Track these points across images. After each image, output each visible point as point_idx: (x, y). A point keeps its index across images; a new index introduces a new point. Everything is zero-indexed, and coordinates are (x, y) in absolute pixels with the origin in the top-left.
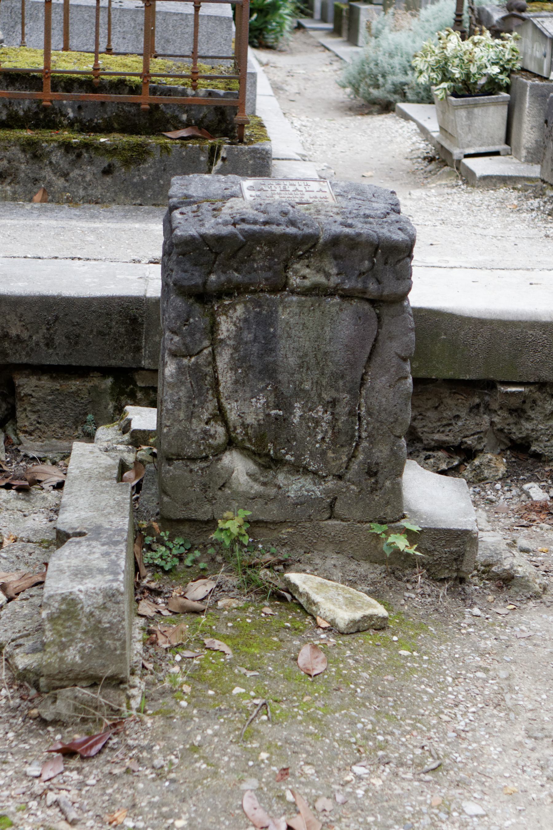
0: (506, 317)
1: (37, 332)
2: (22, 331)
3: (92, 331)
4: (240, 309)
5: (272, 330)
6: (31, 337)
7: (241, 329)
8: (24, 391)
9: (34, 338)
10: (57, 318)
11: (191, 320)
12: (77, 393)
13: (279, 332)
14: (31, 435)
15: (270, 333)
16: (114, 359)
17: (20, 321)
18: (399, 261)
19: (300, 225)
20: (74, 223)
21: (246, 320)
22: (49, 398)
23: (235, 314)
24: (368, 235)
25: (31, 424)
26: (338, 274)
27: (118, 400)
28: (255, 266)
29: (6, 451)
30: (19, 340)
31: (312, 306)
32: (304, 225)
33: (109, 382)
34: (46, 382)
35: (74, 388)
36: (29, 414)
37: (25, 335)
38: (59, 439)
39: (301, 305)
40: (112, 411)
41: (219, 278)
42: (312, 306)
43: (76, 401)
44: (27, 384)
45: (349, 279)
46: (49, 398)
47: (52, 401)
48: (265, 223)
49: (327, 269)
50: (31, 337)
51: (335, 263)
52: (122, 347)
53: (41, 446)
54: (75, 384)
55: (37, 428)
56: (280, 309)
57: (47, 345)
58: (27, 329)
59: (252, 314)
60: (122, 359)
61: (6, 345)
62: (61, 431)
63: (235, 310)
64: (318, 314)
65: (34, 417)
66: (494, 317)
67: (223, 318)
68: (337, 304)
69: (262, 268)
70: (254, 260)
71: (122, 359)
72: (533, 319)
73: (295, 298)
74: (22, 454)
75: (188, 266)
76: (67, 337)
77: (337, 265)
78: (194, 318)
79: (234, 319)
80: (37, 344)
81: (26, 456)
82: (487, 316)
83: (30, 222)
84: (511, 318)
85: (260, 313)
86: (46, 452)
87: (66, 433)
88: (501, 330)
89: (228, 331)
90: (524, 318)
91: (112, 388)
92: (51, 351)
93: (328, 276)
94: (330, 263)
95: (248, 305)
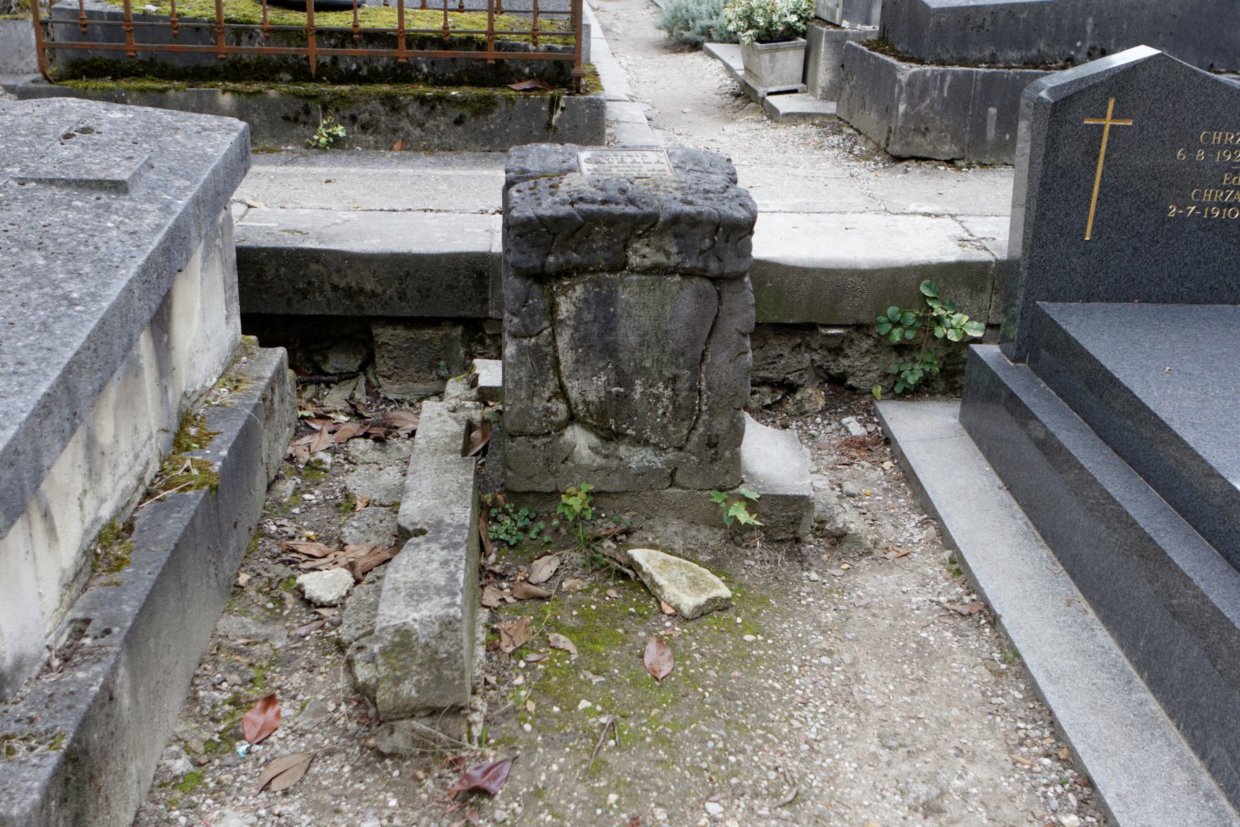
0: (827, 266)
4: (579, 289)
10: (408, 273)
12: (430, 341)
13: (619, 311)
14: (389, 378)
18: (740, 238)
20: (429, 171)
21: (585, 300)
24: (710, 214)
27: (468, 346)
29: (367, 394)
30: (373, 294)
33: (459, 330)
34: (401, 332)
35: (427, 337)
37: (379, 289)
39: (641, 284)
41: (557, 259)
44: (384, 334)
47: (407, 348)
48: (604, 202)
51: (675, 241)
54: (428, 333)
56: (620, 289)
57: (400, 298)
61: (362, 299)
63: (575, 290)
64: (658, 293)
65: (392, 363)
66: (817, 266)
67: (563, 298)
69: (601, 249)
70: (593, 240)
73: (635, 277)
77: (677, 244)
80: (391, 298)
81: (385, 398)
82: (810, 265)
83: (389, 171)
84: (832, 266)
85: (599, 293)
88: (823, 278)
90: (844, 266)
91: (462, 336)
93: (668, 255)
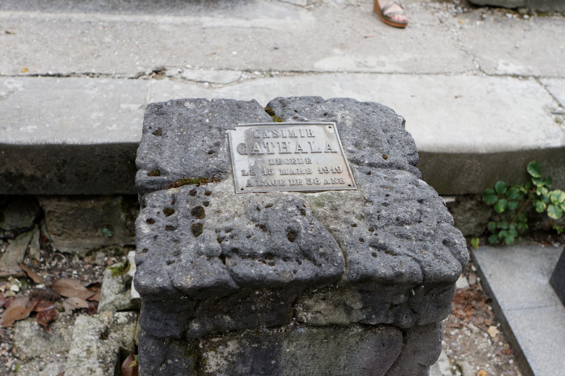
0: (451, 151)
1: (49, 172)
2: (35, 172)
3: (98, 170)
4: (232, 346)
5: (273, 362)
6: (44, 176)
7: (234, 363)
8: (47, 209)
9: (47, 176)
10: (65, 162)
11: (170, 362)
12: (93, 209)
13: (282, 363)
14: (60, 235)
15: (271, 365)
16: (121, 189)
17: (32, 164)
18: (444, 291)
19: (316, 257)
20: (99, 16)
21: (240, 355)
22: (71, 212)
23: (227, 350)
24: (412, 274)
25: (58, 230)
26: (361, 310)
27: (128, 211)
28: (253, 308)
29: (41, 248)
30: (32, 178)
31: (326, 338)
32: (322, 255)
33: (119, 200)
35: (90, 206)
36: (56, 223)
37: (39, 174)
38: (83, 238)
39: (311, 338)
40: (124, 219)
41: (203, 325)
42: (326, 338)
43: (93, 214)
44: (49, 206)
45: (377, 314)
46: (71, 212)
47: (73, 214)
48: (269, 256)
49: (348, 303)
50: (44, 176)
51: (360, 296)
52: (126, 181)
53: (70, 244)
54: (91, 204)
55: (64, 232)
56: (285, 343)
57: (60, 181)
58: (39, 170)
59: (249, 349)
60: (128, 189)
61: (23, 182)
62: (84, 233)
63: (227, 346)
64: (332, 345)
65: (60, 225)
66: (441, 151)
67: (211, 354)
68: (358, 334)
69: (262, 311)
70: (252, 302)
71: (128, 189)
72: (473, 151)
73: (302, 330)
74: (54, 250)
75: (159, 314)
76: (77, 175)
77: (362, 300)
78: (172, 359)
79: (226, 354)
80: (51, 180)
81: (58, 251)
82: (435, 150)
83: (64, 15)
84: (454, 151)
85: (259, 348)
86: (74, 247)
87: (89, 234)
88: (445, 161)
89: (218, 365)
90: (465, 151)
91: (122, 204)
92: (64, 185)
93: (349, 310)
94: (353, 296)
95: (244, 341)
